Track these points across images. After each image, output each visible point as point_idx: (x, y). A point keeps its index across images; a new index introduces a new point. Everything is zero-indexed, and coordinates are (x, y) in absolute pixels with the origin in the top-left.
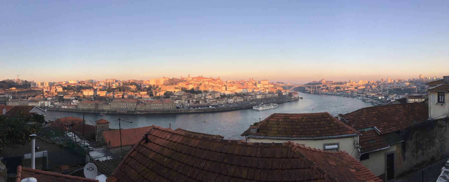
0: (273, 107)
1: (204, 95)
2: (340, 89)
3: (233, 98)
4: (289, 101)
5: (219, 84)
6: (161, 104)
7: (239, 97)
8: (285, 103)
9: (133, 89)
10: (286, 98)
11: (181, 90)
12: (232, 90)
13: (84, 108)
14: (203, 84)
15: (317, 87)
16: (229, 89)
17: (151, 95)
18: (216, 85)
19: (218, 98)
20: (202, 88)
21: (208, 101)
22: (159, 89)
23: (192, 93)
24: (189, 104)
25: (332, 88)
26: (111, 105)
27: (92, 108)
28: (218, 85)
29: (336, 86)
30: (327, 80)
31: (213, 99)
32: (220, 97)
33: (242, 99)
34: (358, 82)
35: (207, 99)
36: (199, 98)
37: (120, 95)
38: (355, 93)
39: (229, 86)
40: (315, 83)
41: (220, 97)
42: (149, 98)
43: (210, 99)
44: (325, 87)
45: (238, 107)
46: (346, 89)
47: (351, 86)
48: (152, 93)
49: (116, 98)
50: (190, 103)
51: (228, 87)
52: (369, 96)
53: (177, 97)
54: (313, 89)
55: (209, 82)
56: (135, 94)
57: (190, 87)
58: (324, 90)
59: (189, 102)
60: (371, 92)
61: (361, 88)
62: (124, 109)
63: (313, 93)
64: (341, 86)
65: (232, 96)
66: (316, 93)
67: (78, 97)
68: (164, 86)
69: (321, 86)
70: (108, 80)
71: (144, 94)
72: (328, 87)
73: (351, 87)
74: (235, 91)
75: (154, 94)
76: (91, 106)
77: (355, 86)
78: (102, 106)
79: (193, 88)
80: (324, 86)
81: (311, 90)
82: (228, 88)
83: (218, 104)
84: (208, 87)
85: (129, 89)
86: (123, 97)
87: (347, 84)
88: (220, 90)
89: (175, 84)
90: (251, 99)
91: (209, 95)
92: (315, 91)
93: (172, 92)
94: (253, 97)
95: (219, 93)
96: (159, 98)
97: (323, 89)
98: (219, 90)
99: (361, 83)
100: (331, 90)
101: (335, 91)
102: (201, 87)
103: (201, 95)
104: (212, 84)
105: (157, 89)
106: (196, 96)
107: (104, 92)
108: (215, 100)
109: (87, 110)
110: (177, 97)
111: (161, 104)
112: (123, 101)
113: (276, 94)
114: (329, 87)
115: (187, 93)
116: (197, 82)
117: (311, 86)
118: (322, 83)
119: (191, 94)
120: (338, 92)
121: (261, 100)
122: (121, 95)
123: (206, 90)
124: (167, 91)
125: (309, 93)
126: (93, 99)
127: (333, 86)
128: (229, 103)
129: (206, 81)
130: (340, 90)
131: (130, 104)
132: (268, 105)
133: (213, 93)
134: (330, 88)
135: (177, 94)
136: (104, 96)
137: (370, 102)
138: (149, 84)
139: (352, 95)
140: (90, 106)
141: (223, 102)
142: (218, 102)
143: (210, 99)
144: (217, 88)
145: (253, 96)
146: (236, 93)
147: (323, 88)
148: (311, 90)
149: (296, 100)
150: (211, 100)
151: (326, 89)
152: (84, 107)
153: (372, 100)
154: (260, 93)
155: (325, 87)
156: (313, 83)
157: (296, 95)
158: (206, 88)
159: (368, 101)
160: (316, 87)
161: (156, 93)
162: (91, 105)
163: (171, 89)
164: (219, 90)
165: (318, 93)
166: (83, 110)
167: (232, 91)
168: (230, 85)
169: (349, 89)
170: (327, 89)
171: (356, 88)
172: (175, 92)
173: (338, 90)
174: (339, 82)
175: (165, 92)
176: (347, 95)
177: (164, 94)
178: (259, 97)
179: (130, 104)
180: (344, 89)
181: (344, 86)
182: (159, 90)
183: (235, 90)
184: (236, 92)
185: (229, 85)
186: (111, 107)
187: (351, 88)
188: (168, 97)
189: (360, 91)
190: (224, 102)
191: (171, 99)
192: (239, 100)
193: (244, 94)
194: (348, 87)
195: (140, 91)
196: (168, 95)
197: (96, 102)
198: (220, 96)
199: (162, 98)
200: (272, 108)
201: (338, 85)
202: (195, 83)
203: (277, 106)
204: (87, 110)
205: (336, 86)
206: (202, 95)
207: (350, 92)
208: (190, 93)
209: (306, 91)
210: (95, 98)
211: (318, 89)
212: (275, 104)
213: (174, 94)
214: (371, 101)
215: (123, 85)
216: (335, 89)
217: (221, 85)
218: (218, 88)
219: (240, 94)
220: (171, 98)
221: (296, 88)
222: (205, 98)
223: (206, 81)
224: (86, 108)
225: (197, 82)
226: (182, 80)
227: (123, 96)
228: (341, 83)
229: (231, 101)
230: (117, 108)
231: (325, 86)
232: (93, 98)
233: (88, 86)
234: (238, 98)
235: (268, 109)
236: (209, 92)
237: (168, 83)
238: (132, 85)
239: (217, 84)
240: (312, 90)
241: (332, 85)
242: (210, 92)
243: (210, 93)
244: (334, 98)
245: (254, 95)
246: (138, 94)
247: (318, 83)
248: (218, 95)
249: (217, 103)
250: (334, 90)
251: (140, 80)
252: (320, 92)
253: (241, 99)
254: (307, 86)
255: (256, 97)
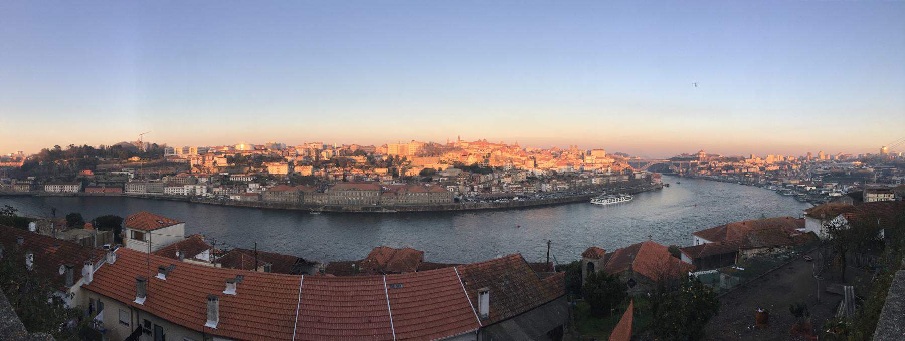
0: (625, 200)
1: (496, 176)
2: (733, 169)
3: (550, 182)
4: (647, 191)
5: (521, 156)
6: (426, 193)
7: (560, 181)
8: (639, 194)
9: (360, 163)
10: (643, 185)
11: (452, 166)
12: (547, 167)
13: (276, 200)
14: (492, 156)
15: (690, 165)
16: (542, 166)
17: (395, 175)
18: (516, 157)
19: (522, 182)
20: (492, 163)
21: (505, 188)
22: (408, 163)
23: (475, 172)
24: (472, 193)
25: (718, 167)
26: (329, 195)
27: (291, 199)
28: (519, 157)
29: (725, 164)
30: (709, 153)
31: (514, 184)
32: (525, 179)
33: (567, 184)
34: (765, 158)
35: (504, 183)
36: (489, 181)
37: (339, 175)
38: (761, 178)
39: (540, 160)
40: (687, 158)
41: (525, 179)
42: (392, 181)
43: (510, 184)
44: (705, 166)
45: (564, 198)
46: (743, 171)
47: (754, 165)
48: (397, 170)
49: (332, 181)
50: (474, 191)
51: (540, 162)
52: (789, 184)
53: (446, 179)
54: (685, 168)
55: (502, 152)
56: (366, 172)
57: (470, 161)
58: (704, 172)
59: (472, 189)
60: (791, 177)
61: (771, 170)
62: (356, 204)
63: (684, 176)
64: (734, 164)
65: (549, 177)
66: (689, 176)
67: (258, 177)
68: (417, 157)
69: (699, 163)
70: (311, 145)
71: (383, 173)
72: (711, 165)
73: (754, 167)
74: (553, 169)
75: (400, 174)
76: (290, 197)
77: (760, 166)
78: (312, 196)
79: (476, 162)
80: (703, 164)
81: (681, 171)
82: (538, 162)
83: (525, 193)
84: (503, 161)
85: (353, 163)
86: (345, 180)
87: (746, 161)
88: (525, 166)
89: (439, 155)
90: (583, 185)
91: (505, 177)
92: (687, 171)
93: (436, 170)
94: (586, 180)
95: (524, 173)
96: (410, 179)
97: (703, 169)
98: (523, 166)
99: (770, 160)
100: (717, 171)
101: (724, 173)
102: (490, 161)
103: (492, 176)
104: (508, 156)
105: (405, 163)
106: (482, 178)
107: (308, 167)
108: (518, 186)
109: (282, 204)
110: (447, 180)
111: (426, 194)
112: (354, 188)
113: (625, 177)
114: (713, 165)
115: (465, 173)
116: (481, 152)
117: (681, 162)
118: (699, 158)
119: (473, 174)
120: (730, 175)
121: (600, 186)
122: (341, 175)
123: (500, 167)
124: (425, 167)
125: (677, 175)
126: (289, 182)
127: (721, 164)
128: (544, 190)
129: (498, 150)
130: (733, 171)
131: (367, 193)
132: (617, 197)
133: (513, 172)
134: (715, 168)
135: (445, 174)
136: (308, 176)
137: (792, 195)
138: (386, 155)
139: (753, 180)
140: (289, 196)
141: (533, 189)
142: (525, 188)
143: (510, 184)
144: (520, 164)
145: (587, 179)
146: (555, 173)
147: (702, 166)
148: (681, 171)
149: (659, 189)
150: (512, 185)
151: (708, 170)
152: (276, 199)
153: (795, 192)
154: (595, 174)
155: (705, 166)
156: (683, 157)
157: (658, 179)
158: (500, 163)
159: (787, 193)
160: (689, 164)
161: (404, 170)
162: (290, 193)
163: (432, 164)
164: (524, 167)
165: (694, 175)
166: (274, 204)
167: (548, 170)
168: (542, 158)
169: (749, 170)
170: (710, 168)
171: (762, 169)
172: (440, 170)
173: (729, 172)
174: (729, 157)
175: (421, 169)
176: (746, 181)
177: (420, 173)
178: (595, 181)
179: (367, 193)
180: (740, 170)
181: (740, 164)
182: (407, 165)
183: (552, 167)
184: (554, 171)
185: (540, 158)
186: (329, 198)
187: (754, 168)
188: (430, 180)
189: (769, 176)
190: (535, 189)
191: (435, 183)
192: (561, 186)
193: (569, 176)
194: (748, 168)
195: (376, 168)
196: (428, 175)
197: (299, 187)
198: (525, 178)
199: (419, 182)
200: (623, 203)
201: (730, 163)
202: (478, 153)
203: (632, 198)
204: (283, 205)
205: (725, 164)
206: (493, 176)
207: (752, 177)
208: (470, 171)
209: (671, 171)
210: (291, 179)
211: (692, 169)
212: (629, 196)
213: (441, 174)
214: (794, 193)
215: (341, 155)
216: (724, 170)
217: (524, 159)
218: (522, 164)
219: (563, 176)
220: (435, 181)
221: (653, 166)
222: (499, 181)
223: (498, 150)
224: (280, 199)
225: (481, 150)
226: (451, 148)
227: (345, 176)
228: (734, 160)
229: (547, 187)
230: (341, 201)
231: (706, 163)
232: (289, 180)
233: (274, 155)
234: (560, 182)
235: (617, 204)
236: (506, 171)
237: (425, 152)
238: (358, 155)
239: (516, 154)
240: (683, 170)
241: (719, 163)
242: (506, 170)
243: (508, 172)
244: (721, 186)
245: (587, 177)
246: (372, 172)
247: (692, 157)
248: (522, 176)
249: (523, 190)
250: (721, 171)
251: (370, 145)
252: (696, 175)
253: (564, 184)
254: (673, 162)
255: (591, 180)
